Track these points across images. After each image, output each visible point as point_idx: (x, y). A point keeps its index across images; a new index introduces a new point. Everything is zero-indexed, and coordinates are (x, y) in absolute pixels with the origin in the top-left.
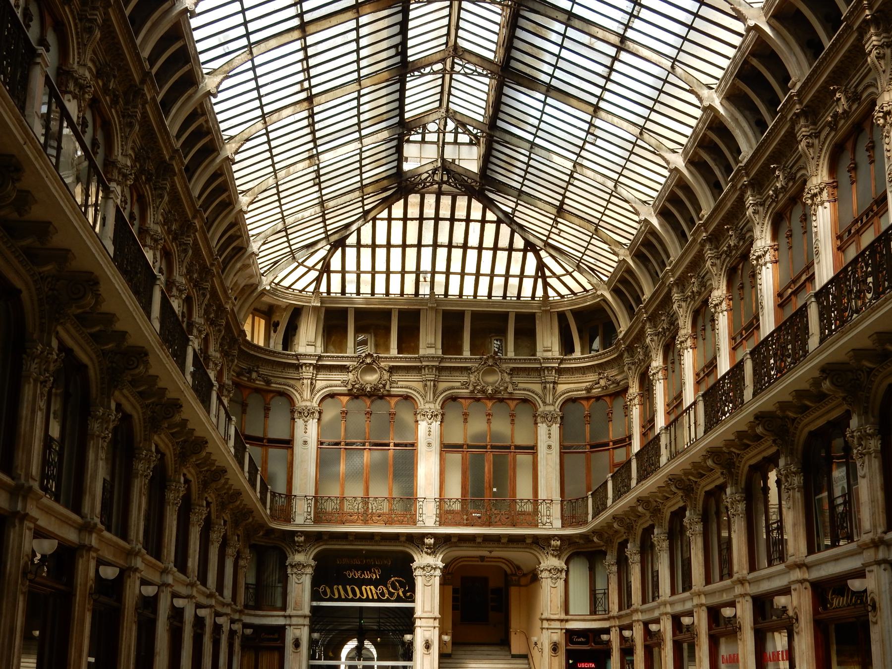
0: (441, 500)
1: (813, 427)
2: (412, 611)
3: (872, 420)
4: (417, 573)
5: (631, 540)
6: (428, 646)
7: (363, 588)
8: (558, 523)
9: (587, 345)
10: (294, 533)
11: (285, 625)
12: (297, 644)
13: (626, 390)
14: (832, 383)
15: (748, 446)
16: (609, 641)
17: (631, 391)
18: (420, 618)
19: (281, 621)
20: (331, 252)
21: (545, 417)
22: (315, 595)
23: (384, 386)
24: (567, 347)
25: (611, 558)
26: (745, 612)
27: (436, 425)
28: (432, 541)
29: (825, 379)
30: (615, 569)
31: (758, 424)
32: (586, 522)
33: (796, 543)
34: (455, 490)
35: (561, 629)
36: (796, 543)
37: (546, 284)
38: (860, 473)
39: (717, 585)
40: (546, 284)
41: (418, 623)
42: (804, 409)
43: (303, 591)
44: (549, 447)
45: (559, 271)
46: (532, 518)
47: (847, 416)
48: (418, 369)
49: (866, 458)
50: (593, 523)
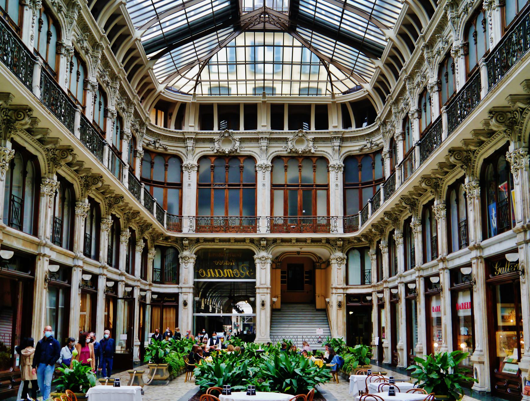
0: (272, 217)
1: (486, 156)
2: (255, 282)
3: (524, 145)
4: (257, 261)
5: (382, 239)
6: (263, 305)
7: (225, 270)
8: (341, 230)
10: (182, 239)
11: (178, 293)
12: (185, 304)
13: (382, 149)
14: (497, 121)
15: (447, 173)
16: (371, 301)
18: (259, 288)
19: (175, 291)
20: (201, 69)
22: (197, 275)
23: (236, 150)
24: (347, 124)
25: (372, 251)
26: (445, 279)
27: (268, 174)
28: (265, 242)
29: (492, 118)
30: (375, 257)
31: (451, 156)
32: (357, 230)
33: (475, 232)
34: (279, 212)
35: (344, 294)
36: (475, 232)
38: (516, 181)
39: (430, 263)
41: (257, 291)
42: (481, 143)
43: (189, 272)
44: (337, 185)
46: (326, 228)
47: (508, 144)
48: (257, 140)
49: (519, 171)
50: (362, 229)
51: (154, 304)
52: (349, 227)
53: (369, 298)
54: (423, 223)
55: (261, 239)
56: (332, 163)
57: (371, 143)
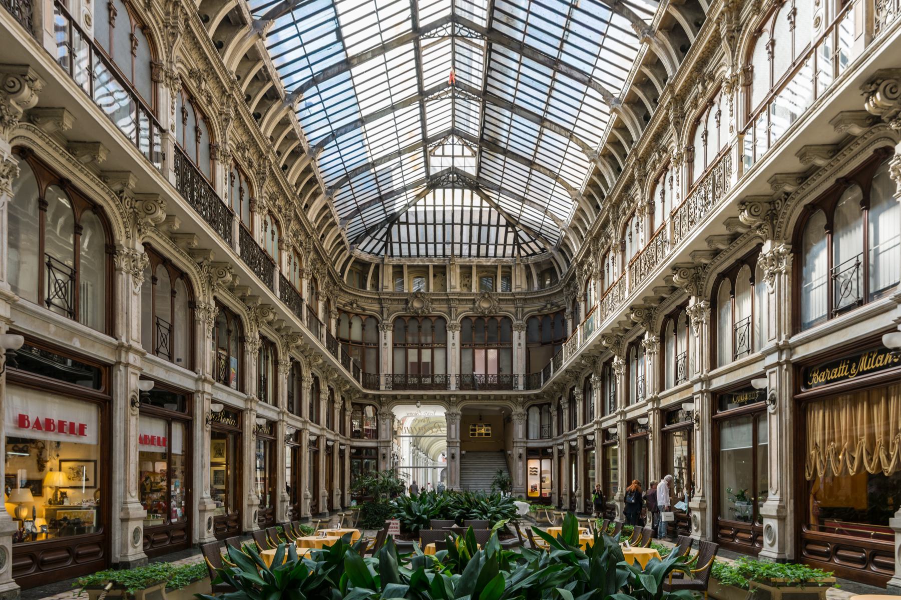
9: (542, 285)
10: (379, 396)
13: (564, 310)
17: (567, 311)
21: (517, 327)
37: (520, 247)
40: (520, 247)
44: (520, 344)
45: (527, 239)
50: (544, 386)
51: (352, 457)
52: (528, 386)
53: (549, 451)
54: (603, 379)
55: (450, 396)
56: (515, 322)
57: (552, 305)
